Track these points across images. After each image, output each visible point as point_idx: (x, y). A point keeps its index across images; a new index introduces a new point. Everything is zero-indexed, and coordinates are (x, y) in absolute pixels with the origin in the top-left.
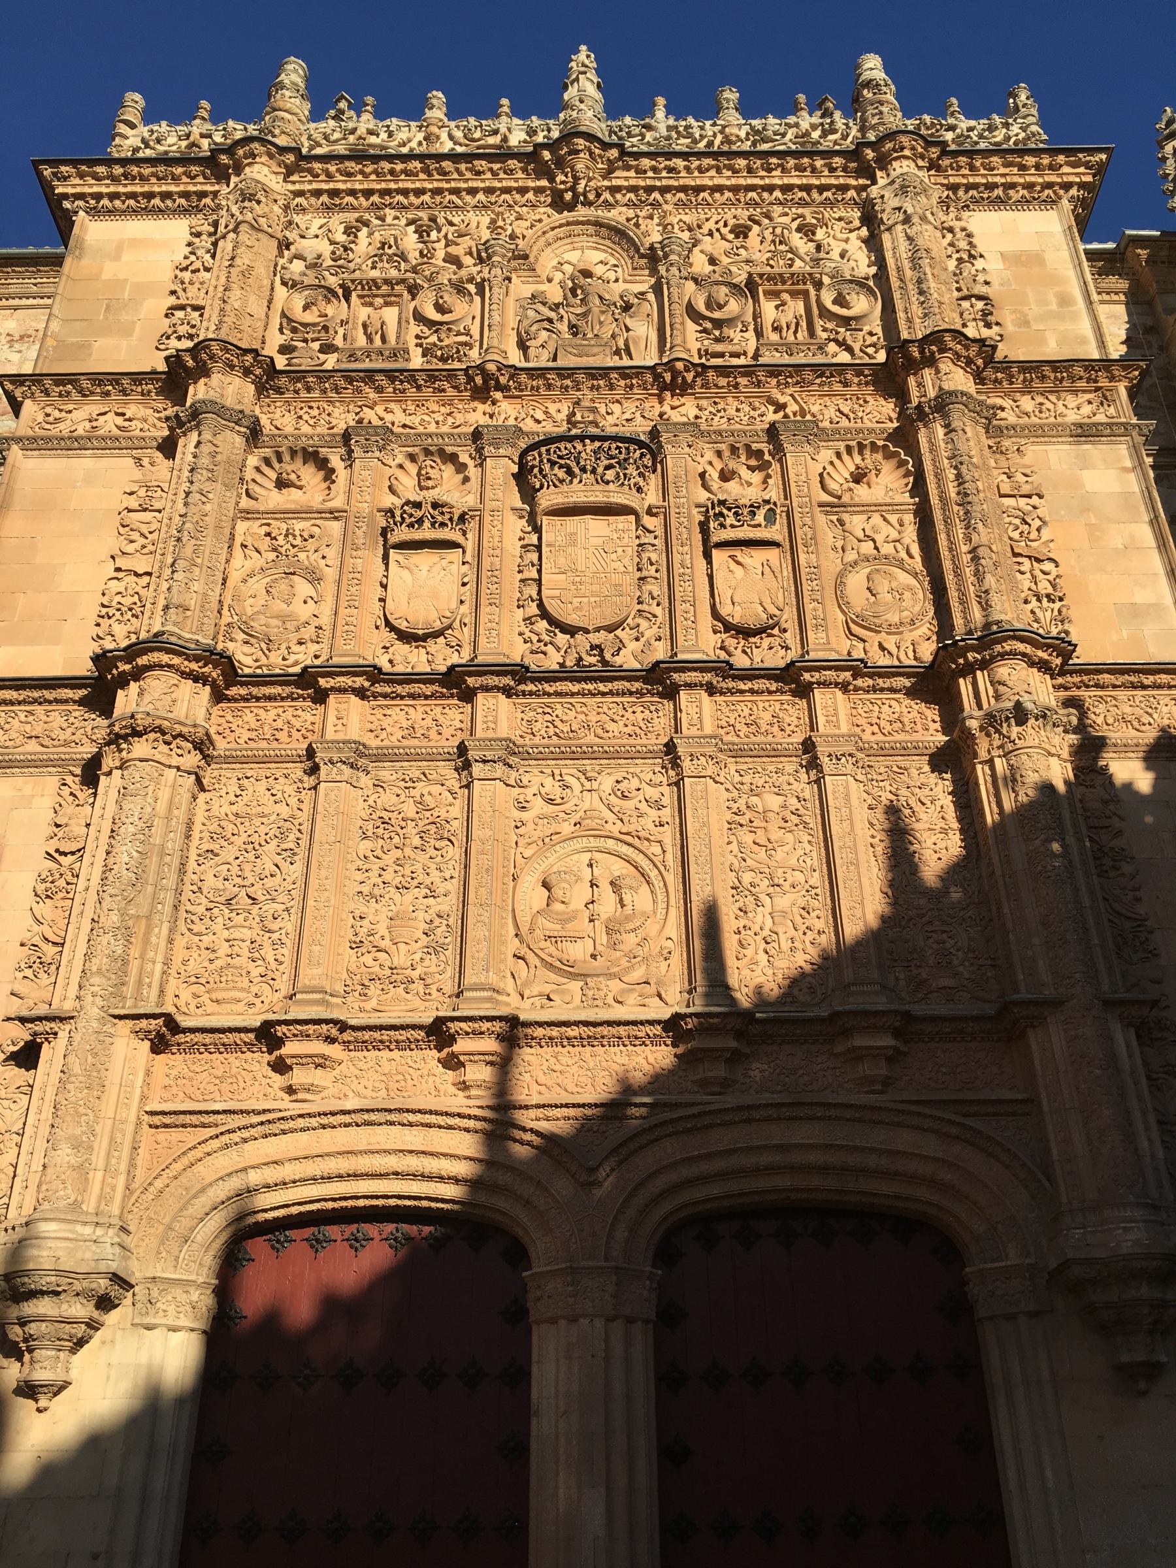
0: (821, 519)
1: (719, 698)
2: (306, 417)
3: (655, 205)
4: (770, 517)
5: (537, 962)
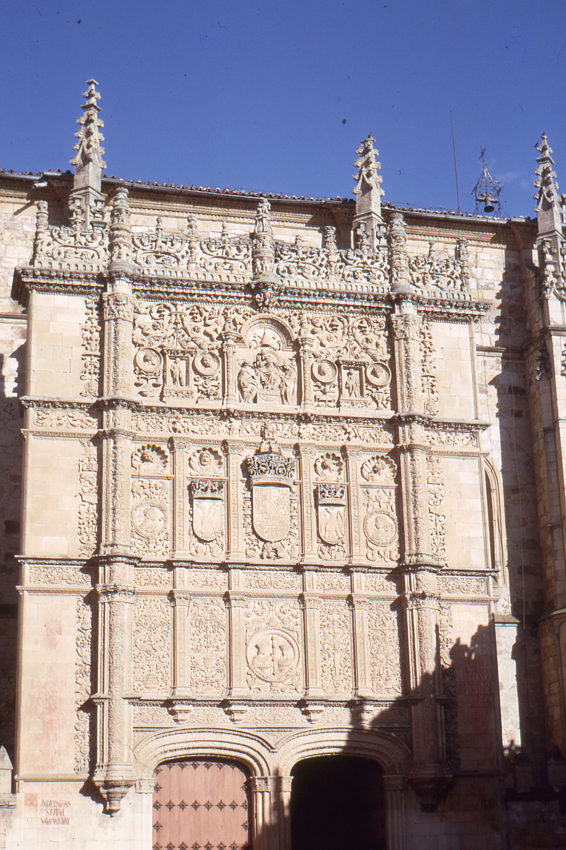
0: (360, 490)
1: (318, 573)
2: (151, 423)
5: (256, 677)
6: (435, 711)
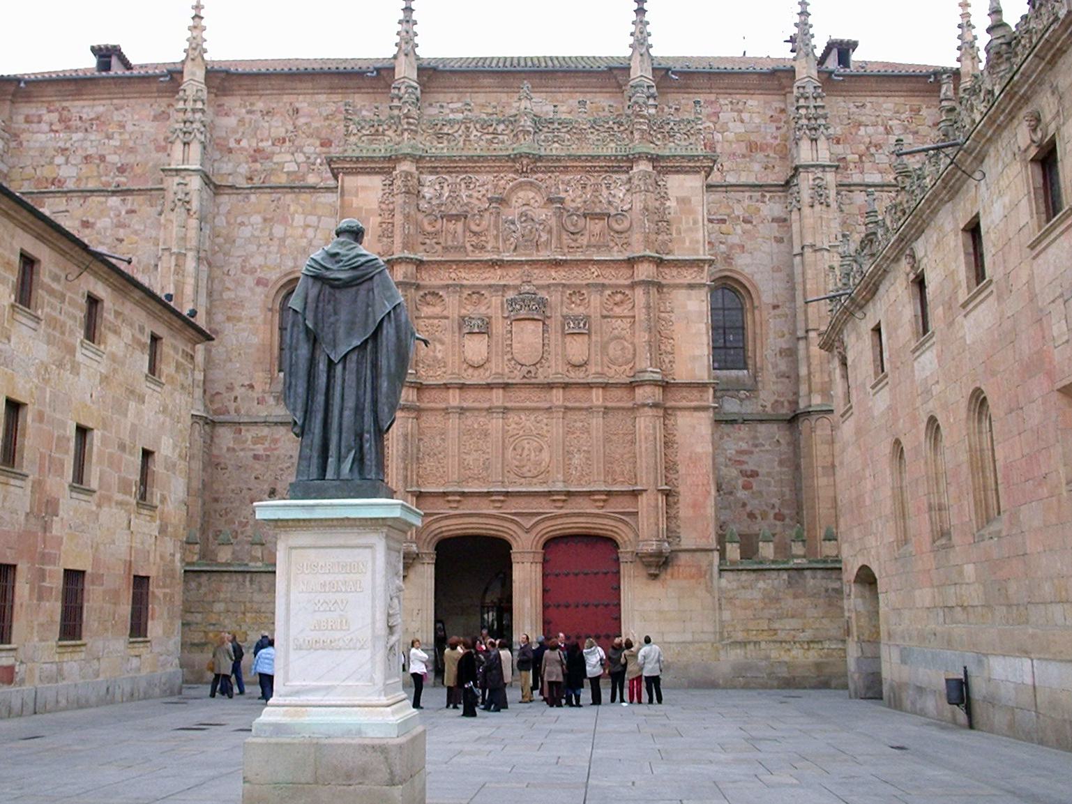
3: (553, 172)
4: (585, 325)
6: (657, 500)
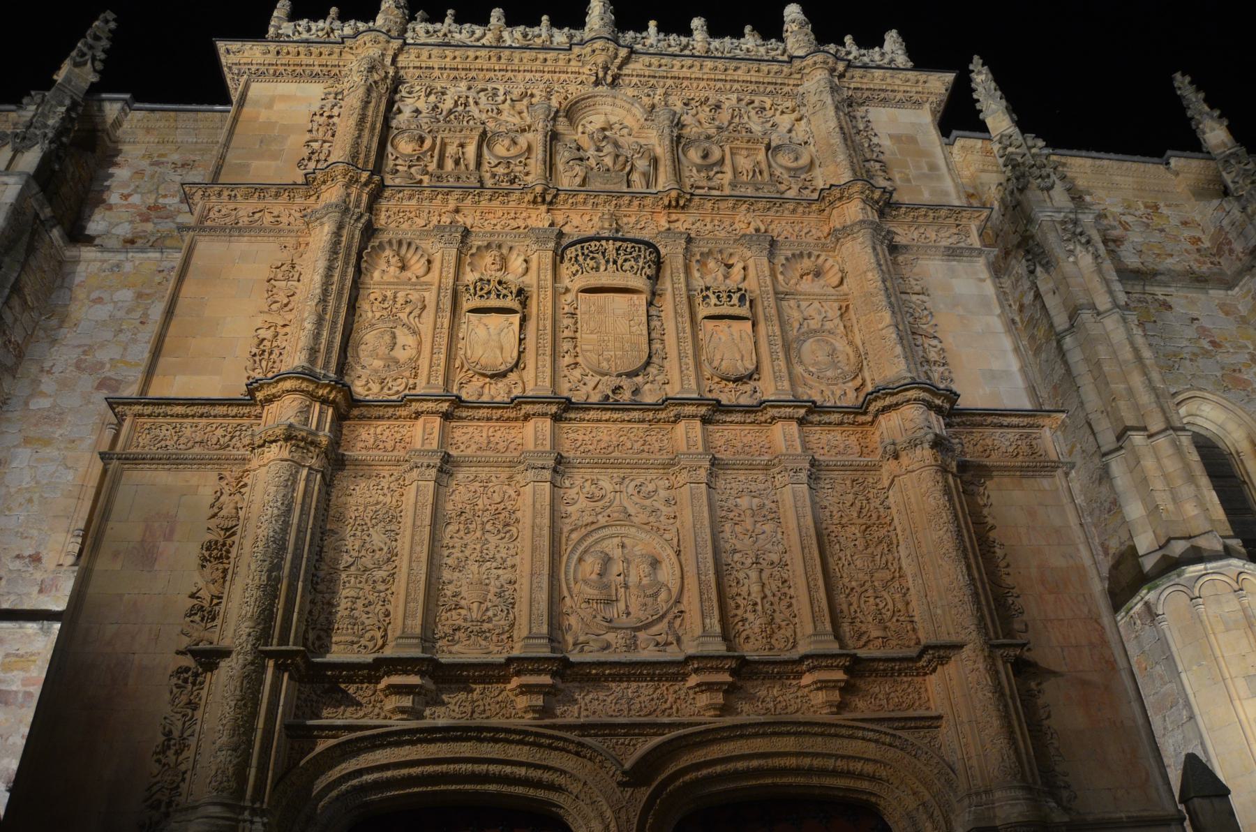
1: (710, 427)
